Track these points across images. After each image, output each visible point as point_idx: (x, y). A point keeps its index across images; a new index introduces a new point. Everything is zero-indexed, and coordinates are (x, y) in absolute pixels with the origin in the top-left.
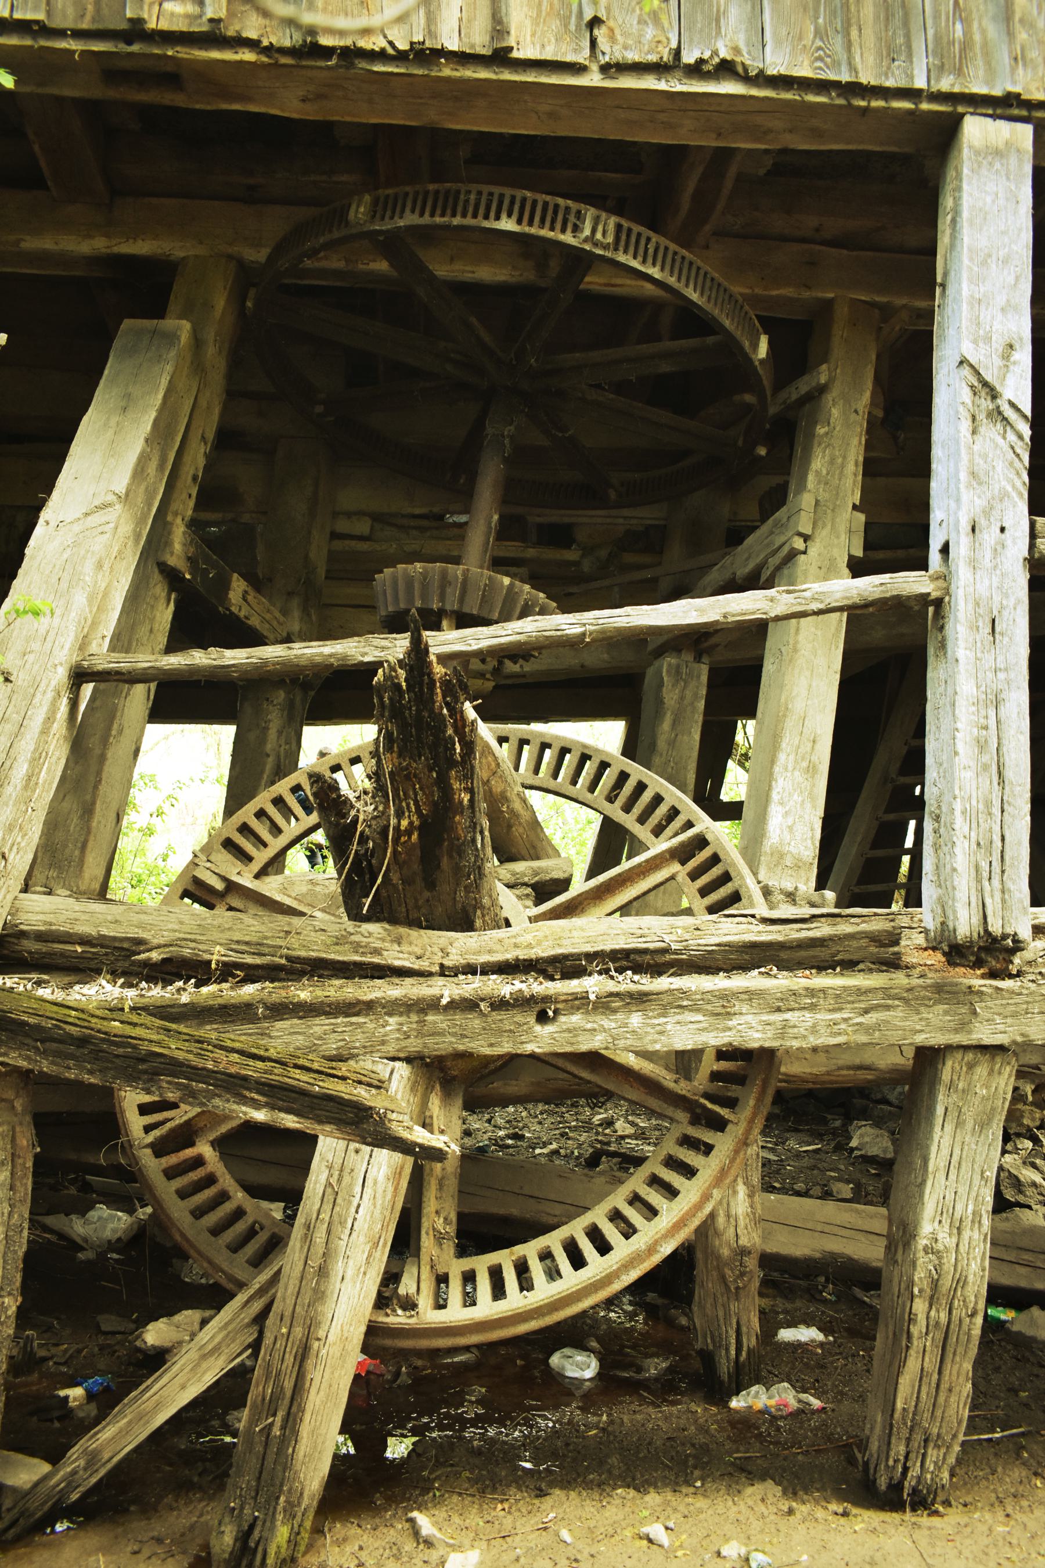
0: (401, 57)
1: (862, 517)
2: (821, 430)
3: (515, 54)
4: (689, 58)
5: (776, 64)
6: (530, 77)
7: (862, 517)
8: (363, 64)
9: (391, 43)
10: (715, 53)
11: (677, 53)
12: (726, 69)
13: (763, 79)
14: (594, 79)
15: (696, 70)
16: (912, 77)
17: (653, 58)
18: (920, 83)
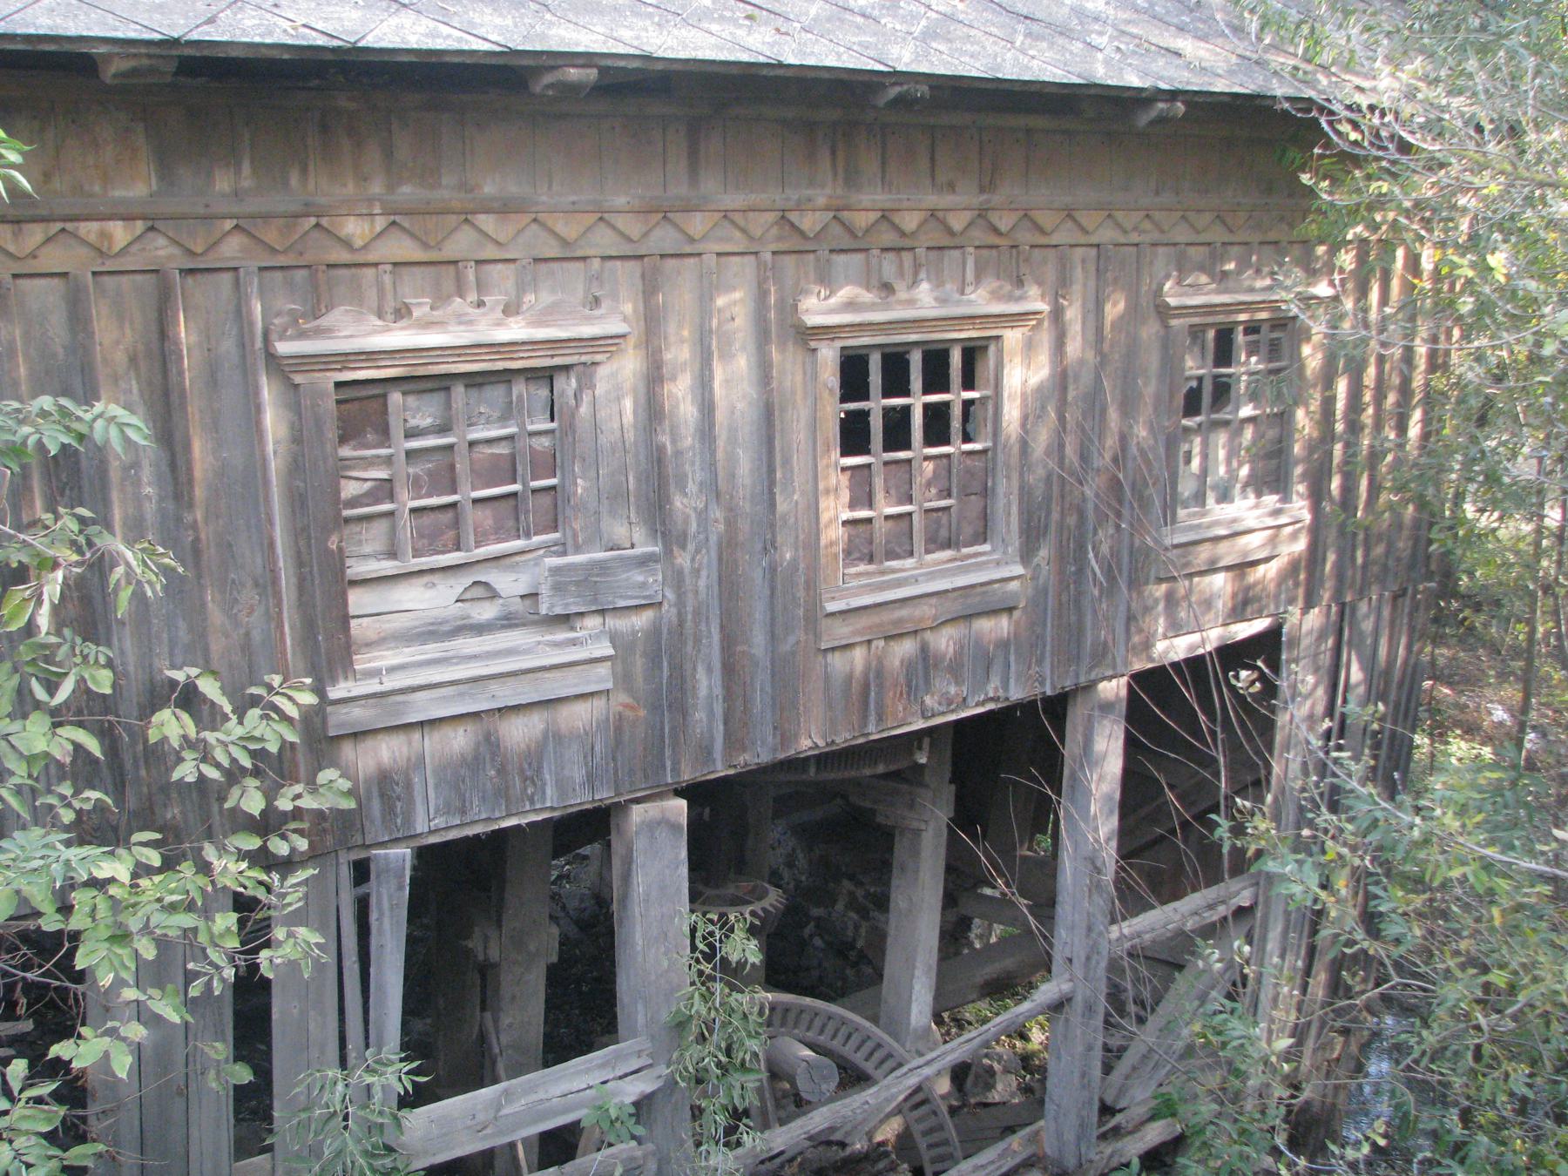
1: (953, 787)
7: (953, 787)
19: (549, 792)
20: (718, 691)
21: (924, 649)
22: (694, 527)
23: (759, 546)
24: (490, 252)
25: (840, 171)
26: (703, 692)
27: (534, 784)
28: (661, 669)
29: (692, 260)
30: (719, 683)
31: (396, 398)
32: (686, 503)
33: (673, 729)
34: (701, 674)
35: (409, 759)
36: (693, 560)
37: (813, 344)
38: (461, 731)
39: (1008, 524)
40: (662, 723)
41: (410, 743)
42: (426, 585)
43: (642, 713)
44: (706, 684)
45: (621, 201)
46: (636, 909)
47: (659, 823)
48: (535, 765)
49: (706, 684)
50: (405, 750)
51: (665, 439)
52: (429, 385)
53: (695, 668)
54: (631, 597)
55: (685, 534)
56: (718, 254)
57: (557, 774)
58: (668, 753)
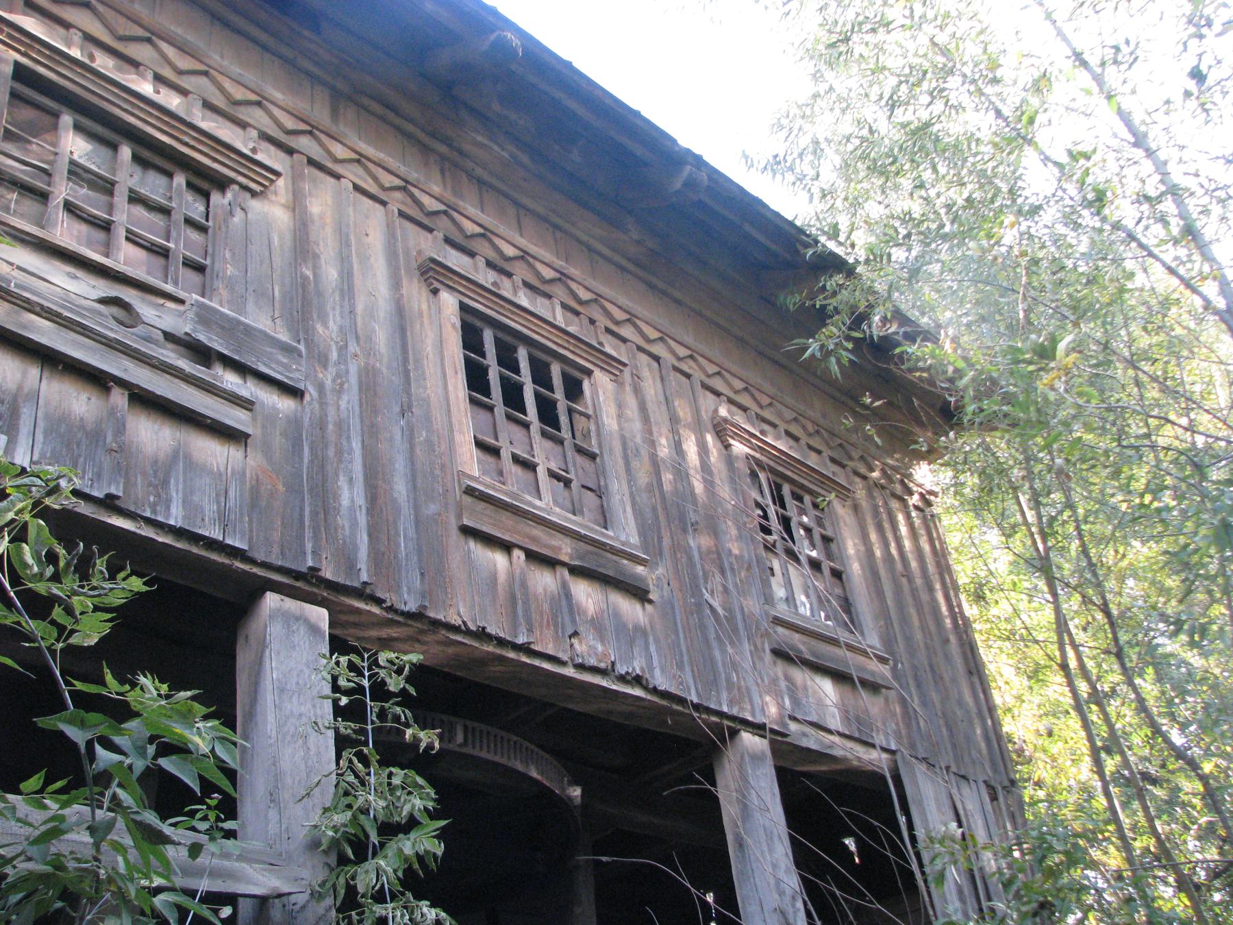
0: (468, 633)
2: (578, 910)
3: (532, 646)
4: (622, 669)
5: (662, 683)
6: (536, 662)
8: (443, 632)
9: (464, 622)
10: (634, 669)
11: (613, 664)
12: (638, 680)
13: (655, 691)
14: (569, 672)
15: (622, 679)
16: (721, 705)
17: (603, 665)
18: (725, 709)
19: (174, 510)
20: (361, 501)
21: (568, 596)
22: (334, 355)
23: (397, 409)
24: (167, 73)
25: (449, 186)
26: (345, 502)
27: (158, 496)
28: (301, 458)
29: (332, 180)
30: (362, 493)
31: (67, 119)
32: (328, 330)
33: (314, 514)
34: (342, 481)
35: (20, 388)
36: (334, 381)
37: (436, 285)
38: (84, 396)
39: (626, 518)
40: (302, 509)
41: (24, 374)
42: (68, 274)
43: (281, 488)
44: (350, 495)
45: (278, 96)
46: (268, 697)
47: (297, 619)
48: (161, 475)
49: (350, 495)
50: (19, 376)
51: (309, 273)
52: (99, 129)
53: (337, 475)
54: (274, 370)
55: (327, 360)
56: (357, 188)
57: (185, 494)
58: (308, 533)
